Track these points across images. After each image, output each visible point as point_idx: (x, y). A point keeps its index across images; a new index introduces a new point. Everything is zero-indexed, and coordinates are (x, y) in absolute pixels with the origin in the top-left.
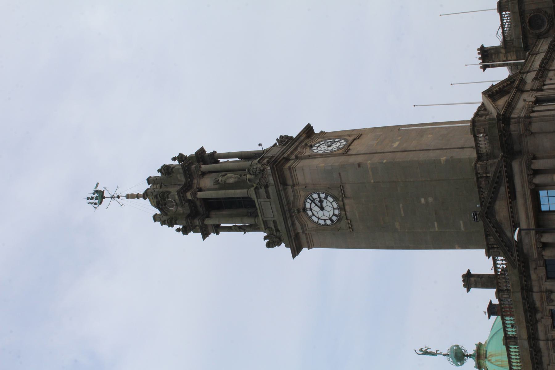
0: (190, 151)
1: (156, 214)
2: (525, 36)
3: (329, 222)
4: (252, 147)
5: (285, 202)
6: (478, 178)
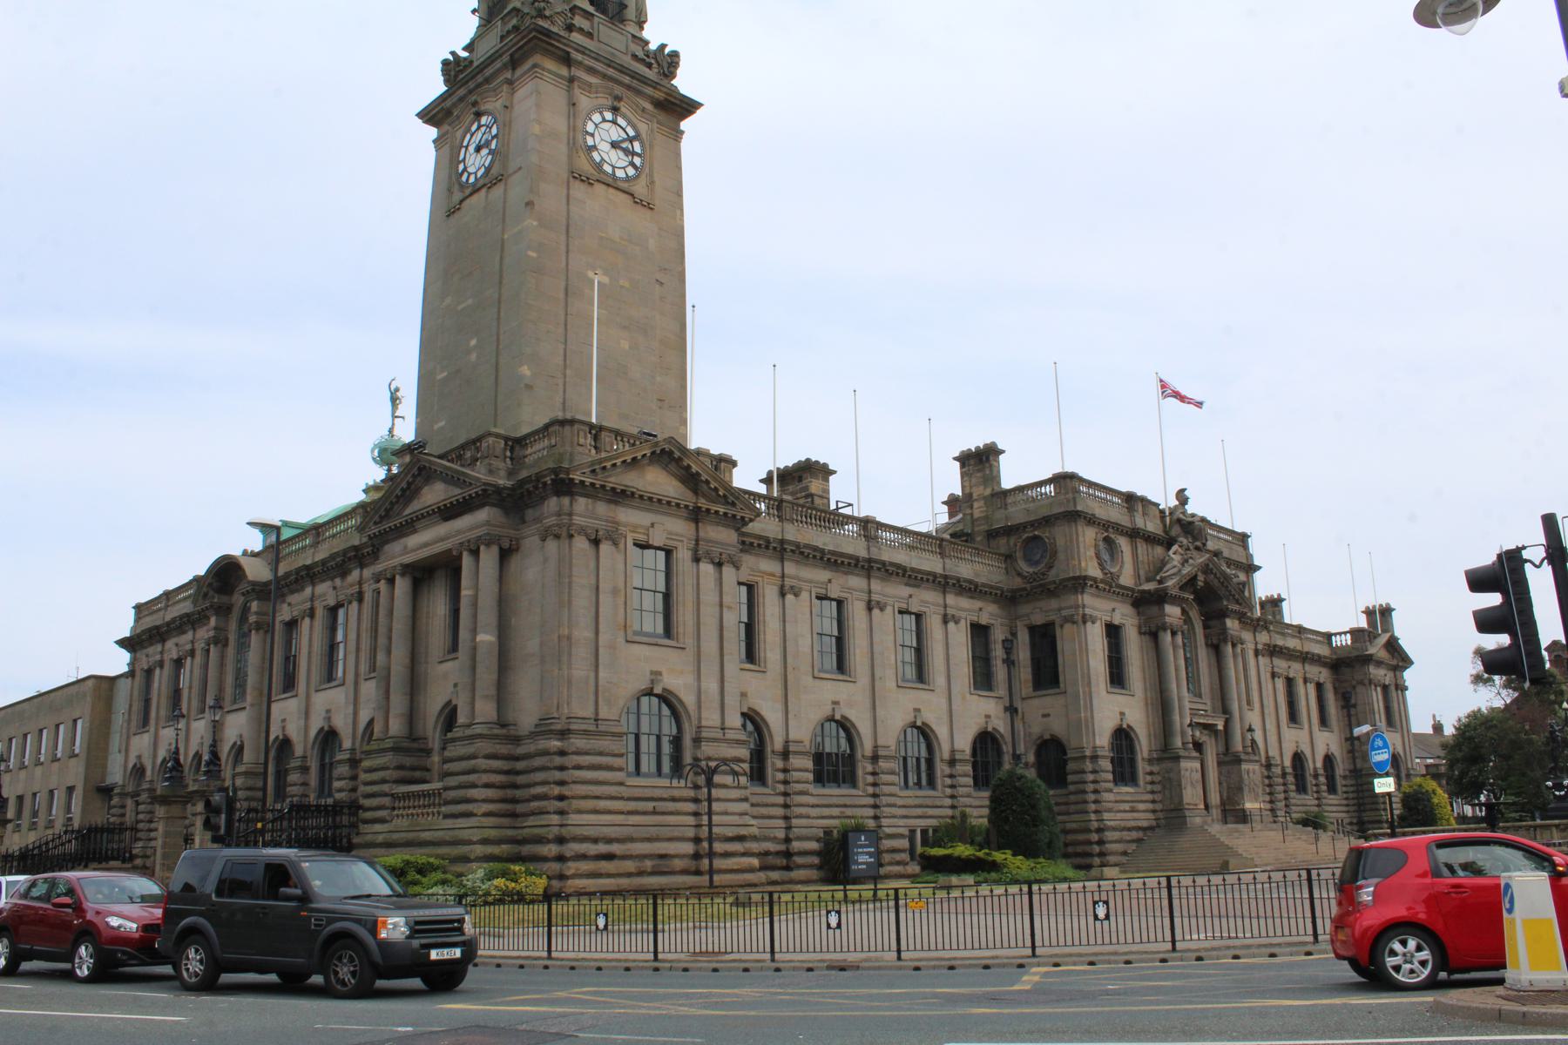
2: (1009, 531)
3: (461, 167)
5: (488, 72)
6: (474, 442)
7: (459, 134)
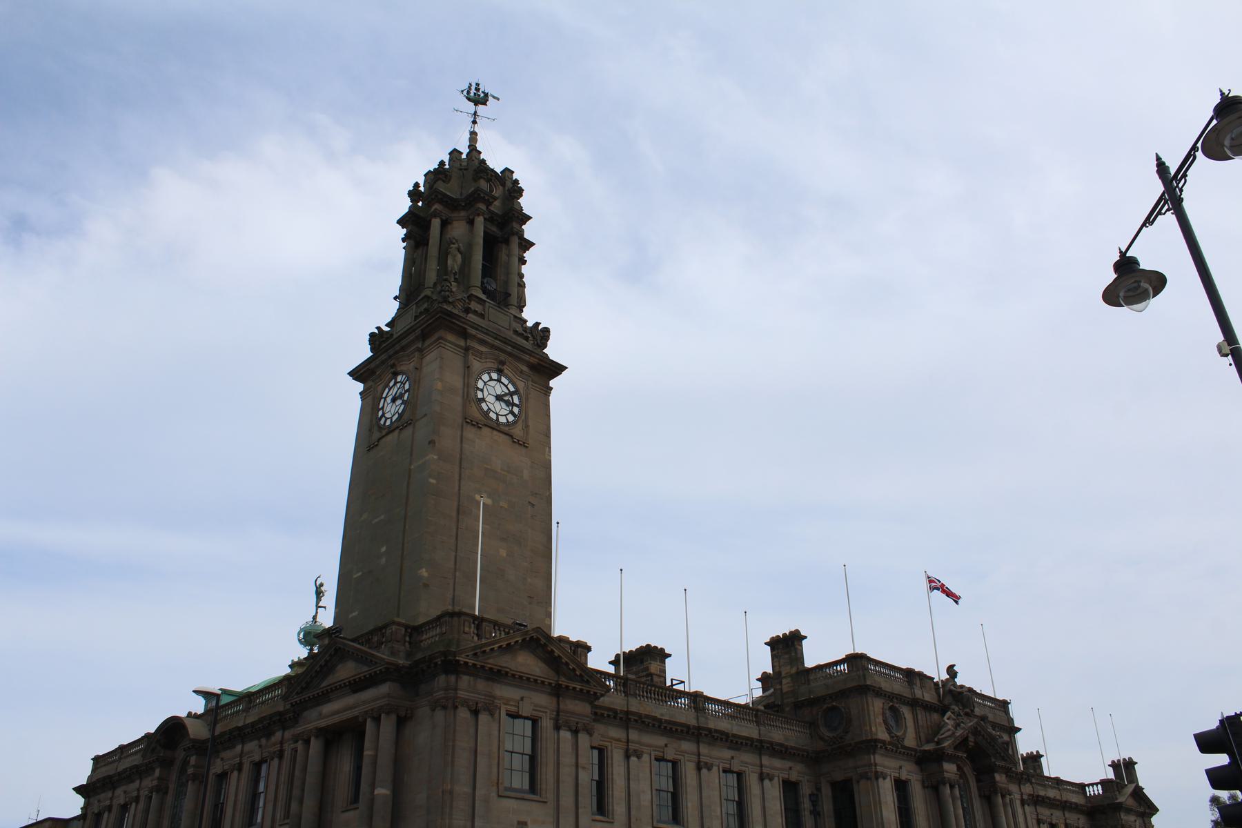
2: (813, 702)
3: (380, 413)
5: (404, 342)
7: (381, 387)
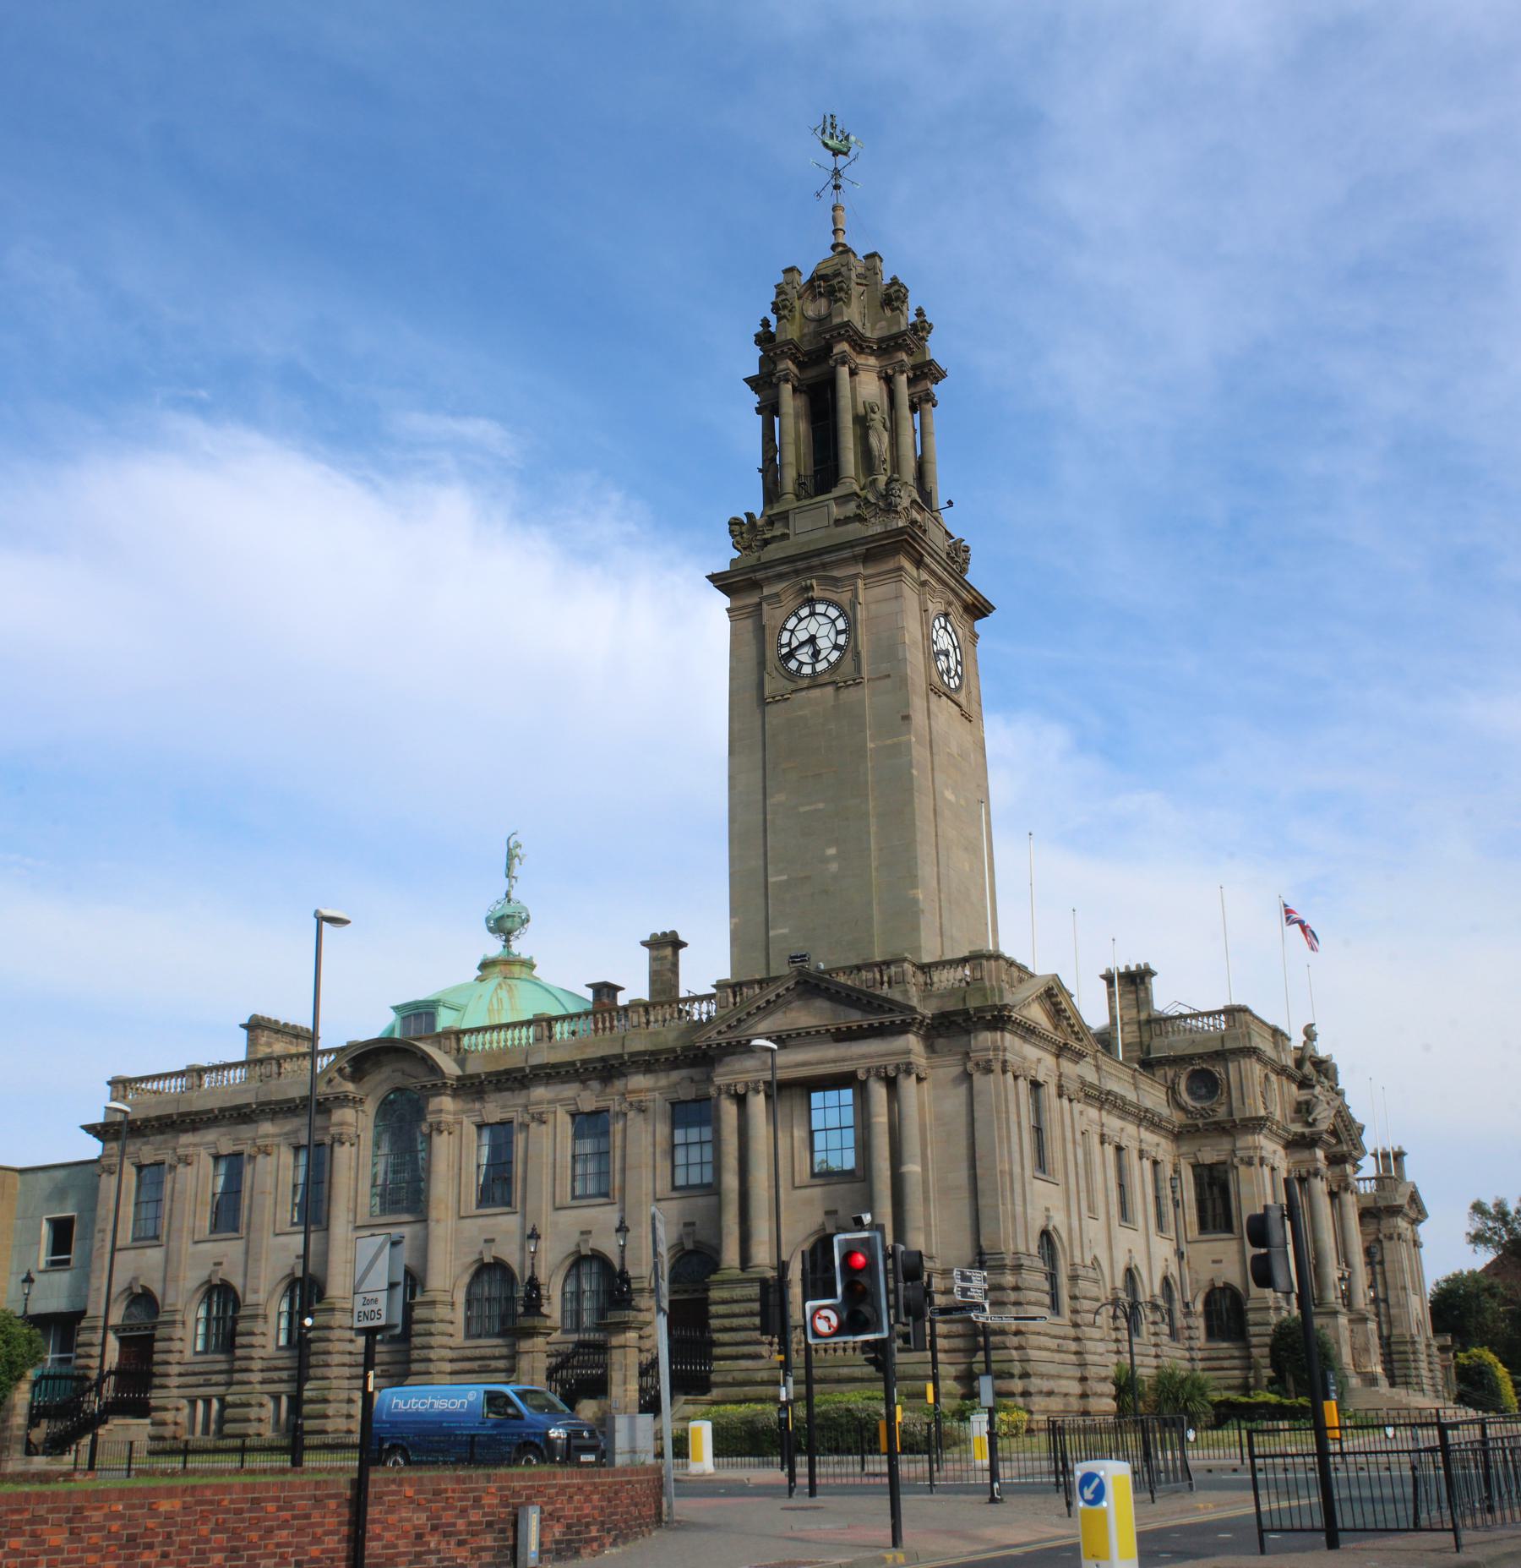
0: (937, 348)
1: (800, 274)
3: (785, 651)
4: (943, 487)
5: (827, 558)
6: (879, 965)
